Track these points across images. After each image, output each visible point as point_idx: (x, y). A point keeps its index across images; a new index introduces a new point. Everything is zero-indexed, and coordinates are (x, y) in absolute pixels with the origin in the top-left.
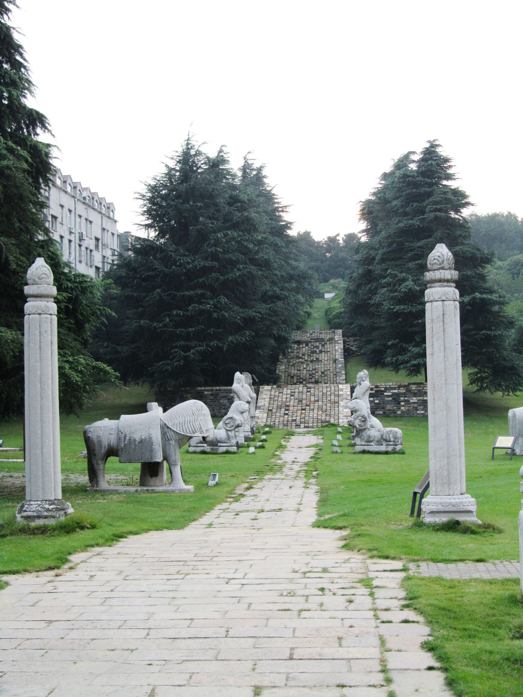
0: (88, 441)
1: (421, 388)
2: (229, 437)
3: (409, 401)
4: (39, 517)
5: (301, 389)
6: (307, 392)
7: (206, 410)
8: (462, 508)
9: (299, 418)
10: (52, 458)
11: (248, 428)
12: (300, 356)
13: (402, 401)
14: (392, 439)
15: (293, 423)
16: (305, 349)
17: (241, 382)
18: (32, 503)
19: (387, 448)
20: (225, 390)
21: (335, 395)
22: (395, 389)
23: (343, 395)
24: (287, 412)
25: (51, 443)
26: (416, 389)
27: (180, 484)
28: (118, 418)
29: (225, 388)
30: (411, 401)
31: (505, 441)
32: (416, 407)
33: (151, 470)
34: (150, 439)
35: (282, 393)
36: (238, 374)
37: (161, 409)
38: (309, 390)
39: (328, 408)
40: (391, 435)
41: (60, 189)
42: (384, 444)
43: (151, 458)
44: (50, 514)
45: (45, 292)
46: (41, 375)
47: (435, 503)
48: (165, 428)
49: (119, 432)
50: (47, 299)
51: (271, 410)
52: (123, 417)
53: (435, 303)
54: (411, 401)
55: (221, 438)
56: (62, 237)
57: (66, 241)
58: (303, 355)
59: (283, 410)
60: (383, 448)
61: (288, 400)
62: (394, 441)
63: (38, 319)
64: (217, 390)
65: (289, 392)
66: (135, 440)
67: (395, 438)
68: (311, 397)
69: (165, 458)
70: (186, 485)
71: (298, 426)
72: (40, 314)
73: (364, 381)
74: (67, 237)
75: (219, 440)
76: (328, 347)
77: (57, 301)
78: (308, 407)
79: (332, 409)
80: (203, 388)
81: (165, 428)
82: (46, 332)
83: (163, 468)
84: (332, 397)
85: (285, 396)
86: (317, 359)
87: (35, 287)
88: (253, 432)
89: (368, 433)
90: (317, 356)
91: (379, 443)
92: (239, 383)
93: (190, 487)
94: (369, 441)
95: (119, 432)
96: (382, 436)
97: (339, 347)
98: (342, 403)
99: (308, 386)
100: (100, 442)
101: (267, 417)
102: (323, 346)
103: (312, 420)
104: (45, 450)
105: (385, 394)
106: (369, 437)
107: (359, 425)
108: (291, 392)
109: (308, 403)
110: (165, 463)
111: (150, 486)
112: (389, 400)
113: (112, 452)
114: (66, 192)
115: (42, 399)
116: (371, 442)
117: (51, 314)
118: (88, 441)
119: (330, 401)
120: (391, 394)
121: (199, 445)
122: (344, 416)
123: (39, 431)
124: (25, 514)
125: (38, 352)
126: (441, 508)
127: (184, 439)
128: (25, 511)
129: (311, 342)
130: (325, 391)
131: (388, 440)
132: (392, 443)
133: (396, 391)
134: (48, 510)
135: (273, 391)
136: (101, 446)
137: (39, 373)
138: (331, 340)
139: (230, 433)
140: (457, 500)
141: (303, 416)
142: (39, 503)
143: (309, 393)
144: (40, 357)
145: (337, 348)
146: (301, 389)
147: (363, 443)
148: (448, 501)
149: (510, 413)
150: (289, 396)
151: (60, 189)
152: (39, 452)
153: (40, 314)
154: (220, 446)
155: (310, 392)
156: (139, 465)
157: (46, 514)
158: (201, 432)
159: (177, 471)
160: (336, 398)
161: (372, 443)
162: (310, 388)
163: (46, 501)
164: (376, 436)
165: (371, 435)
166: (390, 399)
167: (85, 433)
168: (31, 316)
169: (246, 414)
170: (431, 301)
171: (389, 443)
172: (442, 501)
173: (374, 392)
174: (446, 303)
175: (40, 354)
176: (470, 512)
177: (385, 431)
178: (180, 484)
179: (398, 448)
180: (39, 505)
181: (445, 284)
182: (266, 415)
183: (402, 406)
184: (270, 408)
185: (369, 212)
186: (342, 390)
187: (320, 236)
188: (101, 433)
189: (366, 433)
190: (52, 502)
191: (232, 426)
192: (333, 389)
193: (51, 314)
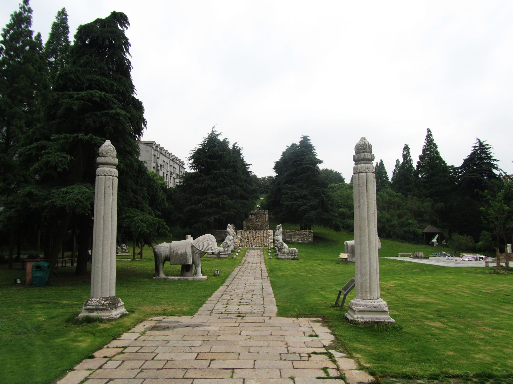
0: (155, 253)
2: (225, 251)
4: (97, 310)
7: (214, 239)
8: (380, 309)
10: (109, 269)
11: (232, 246)
17: (230, 229)
18: (94, 299)
25: (109, 260)
27: (200, 276)
28: (171, 242)
31: (344, 256)
33: (186, 268)
34: (186, 253)
36: (229, 225)
37: (192, 238)
41: (163, 155)
43: (186, 262)
44: (104, 307)
45: (110, 162)
46: (104, 214)
47: (362, 305)
48: (193, 248)
49: (170, 249)
50: (111, 166)
52: (173, 242)
53: (361, 174)
56: (164, 173)
57: (165, 175)
60: (290, 257)
63: (104, 179)
66: (178, 254)
67: (295, 252)
69: (193, 262)
70: (203, 275)
71: (252, 246)
72: (105, 175)
74: (166, 173)
76: (263, 216)
77: (118, 167)
81: (193, 248)
82: (109, 187)
83: (192, 269)
87: (103, 158)
88: (234, 248)
91: (288, 254)
93: (205, 277)
94: (284, 253)
95: (170, 249)
97: (267, 216)
98: (270, 237)
100: (161, 254)
104: (104, 264)
106: (284, 252)
110: (194, 265)
111: (186, 276)
113: (167, 259)
114: (166, 156)
115: (104, 230)
117: (113, 176)
118: (155, 253)
123: (101, 252)
124: (87, 307)
125: (103, 200)
126: (365, 308)
127: (202, 254)
128: (88, 305)
134: (103, 305)
136: (161, 256)
137: (103, 213)
138: (264, 213)
140: (376, 303)
142: (98, 299)
144: (104, 203)
148: (370, 304)
149: (345, 243)
151: (163, 155)
152: (100, 265)
153: (105, 175)
156: (181, 266)
157: (101, 307)
158: (212, 250)
159: (199, 269)
163: (103, 298)
167: (154, 249)
168: (100, 176)
169: (232, 241)
170: (358, 173)
172: (367, 303)
174: (368, 174)
175: (104, 201)
176: (384, 312)
178: (200, 276)
179: (296, 256)
180: (98, 301)
181: (367, 162)
185: (278, 167)
187: (259, 176)
188: (162, 250)
190: (107, 299)
193: (113, 176)
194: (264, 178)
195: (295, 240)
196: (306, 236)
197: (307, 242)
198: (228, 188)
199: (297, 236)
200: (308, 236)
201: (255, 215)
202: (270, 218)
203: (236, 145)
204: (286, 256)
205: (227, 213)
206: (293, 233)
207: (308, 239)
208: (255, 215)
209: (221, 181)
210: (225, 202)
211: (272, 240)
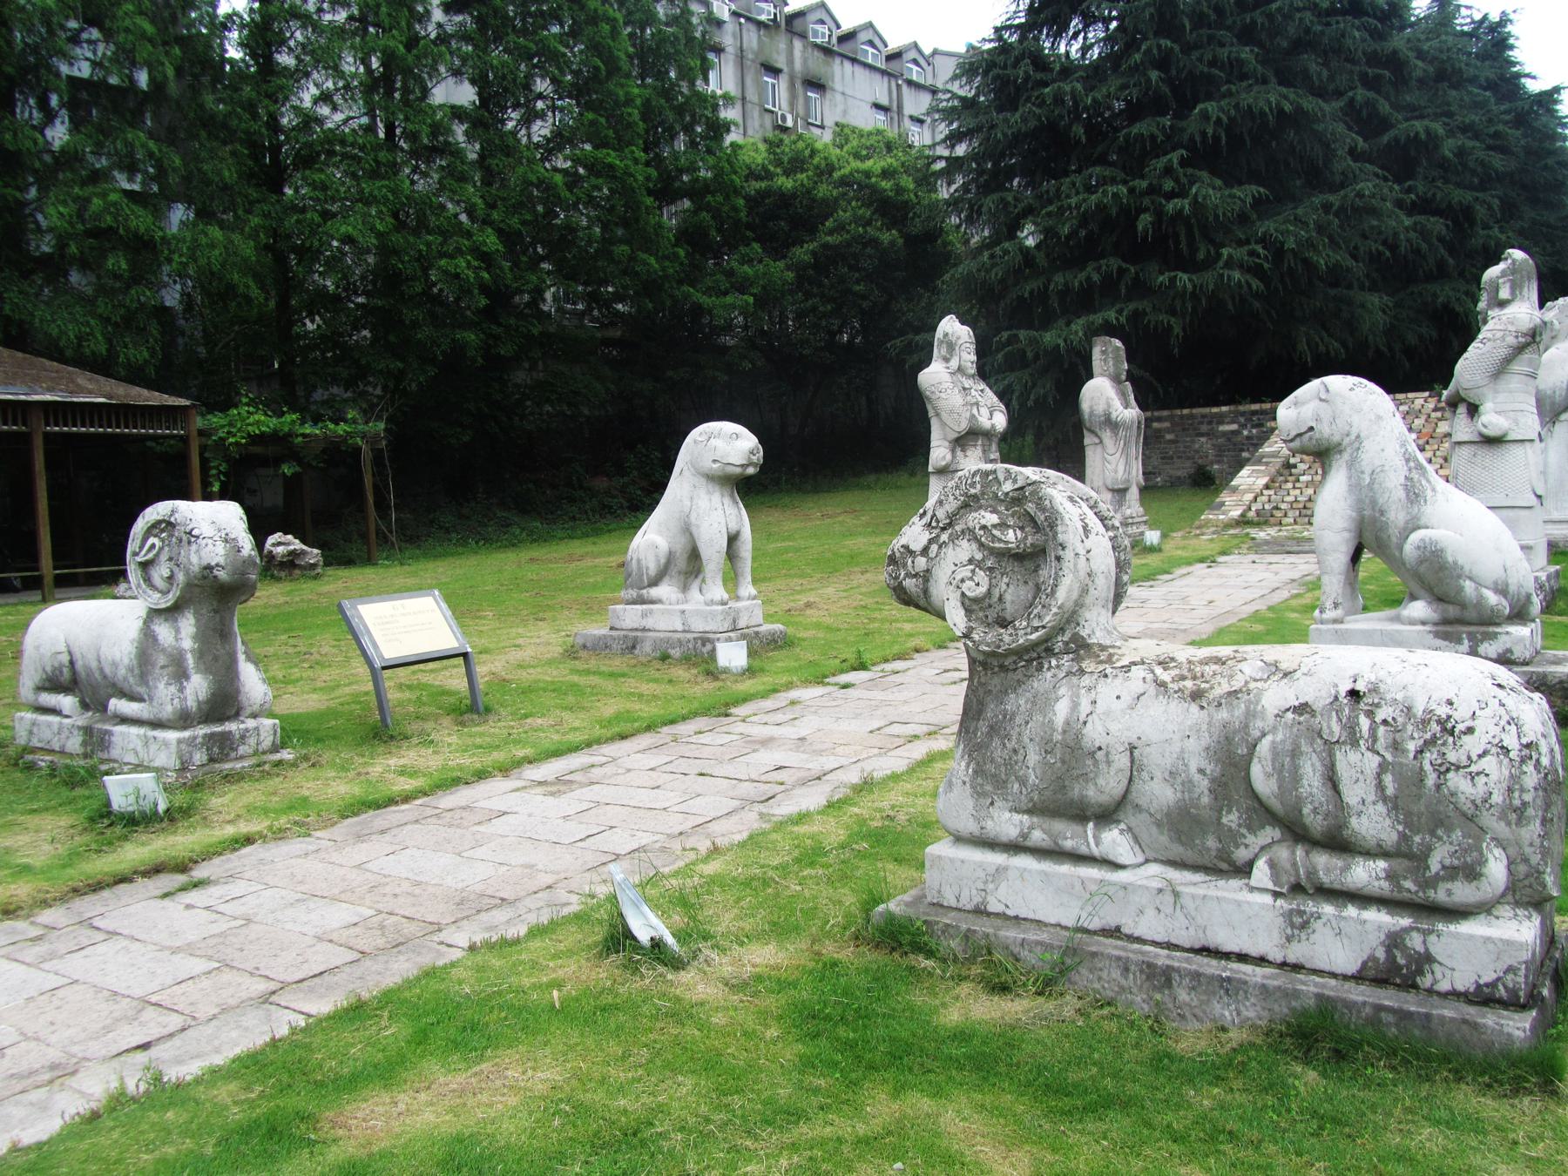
14: (1372, 823)
19: (1299, 925)
20: (1203, 416)
29: (1206, 410)
36: (951, 327)
40: (1357, 766)
42: (1261, 873)
55: (115, 664)
60: (1243, 913)
62: (1407, 856)
64: (1182, 417)
67: (1425, 808)
73: (1502, 304)
75: (108, 670)
89: (1061, 710)
92: (947, 360)
96: (1231, 759)
101: (1267, 487)
106: (1073, 753)
107: (971, 606)
116: (1106, 816)
121: (48, 699)
131: (1315, 822)
132: (1364, 873)
139: (163, 632)
147: (1007, 823)
154: (124, 720)
161: (1114, 841)
164: (1157, 759)
165: (1094, 734)
171: (1325, 865)
177: (1276, 697)
182: (1264, 481)
189: (1044, 703)
191: (171, 578)
198: (1211, 107)
204: (1139, 894)
205: (1183, 278)
209: (1163, 62)
210: (1171, 206)
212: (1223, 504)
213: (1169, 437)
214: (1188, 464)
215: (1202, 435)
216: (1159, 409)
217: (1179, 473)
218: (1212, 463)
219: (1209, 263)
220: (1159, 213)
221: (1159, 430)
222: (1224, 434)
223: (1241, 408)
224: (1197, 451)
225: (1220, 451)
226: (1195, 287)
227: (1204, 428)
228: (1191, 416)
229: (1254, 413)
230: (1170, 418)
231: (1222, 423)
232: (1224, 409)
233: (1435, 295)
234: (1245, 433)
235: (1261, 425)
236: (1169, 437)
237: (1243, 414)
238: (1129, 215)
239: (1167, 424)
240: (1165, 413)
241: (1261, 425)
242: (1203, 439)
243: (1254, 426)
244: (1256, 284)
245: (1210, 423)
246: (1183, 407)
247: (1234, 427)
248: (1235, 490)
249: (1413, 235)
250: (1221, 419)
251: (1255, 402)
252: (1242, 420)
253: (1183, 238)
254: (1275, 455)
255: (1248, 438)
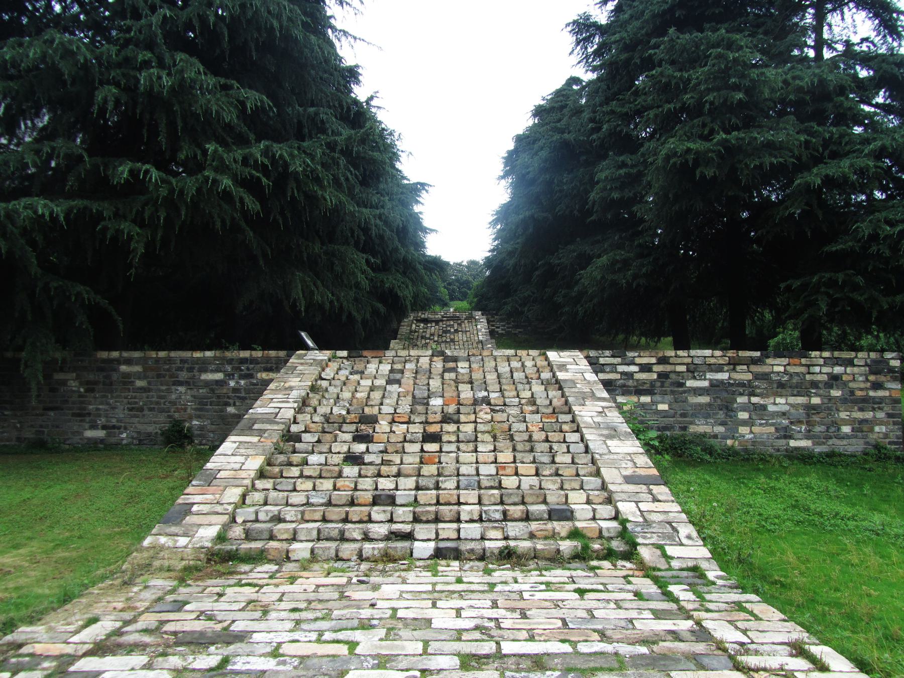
1: (803, 369)
3: (764, 407)
5: (424, 362)
6: (445, 370)
9: (411, 482)
12: (428, 336)
13: (744, 408)
15: (378, 513)
16: (433, 328)
20: (183, 361)
21: (546, 384)
22: (719, 369)
23: (573, 383)
24: (360, 447)
26: (786, 372)
29: (186, 354)
30: (771, 408)
32: (786, 428)
35: (362, 373)
38: (451, 365)
39: (538, 436)
51: (297, 438)
54: (771, 408)
58: (431, 335)
59: (348, 437)
61: (376, 396)
64: (157, 360)
65: (385, 368)
68: (462, 387)
78: (451, 428)
79: (554, 437)
80: (115, 354)
84: (538, 388)
85: (368, 383)
86: (453, 341)
90: (452, 337)
98: (587, 413)
99: (448, 353)
101: (262, 474)
102: (460, 325)
103: (470, 496)
105: (690, 383)
108: (392, 371)
109: (452, 409)
112: (700, 405)
119: (532, 401)
120: (706, 384)
122: (629, 480)
129: (442, 321)
130: (504, 368)
133: (724, 376)
135: (334, 365)
138: (470, 318)
141: (430, 469)
143: (453, 375)
145: (479, 327)
146: (424, 362)
150: (380, 382)
155: (454, 370)
160: (554, 393)
162: (455, 360)
166: (704, 400)
173: (655, 376)
182: (256, 463)
183: (744, 423)
184: (294, 428)
186: (563, 367)
192: (529, 364)
194: (460, 265)
195: (763, 430)
196: (852, 400)
197: (856, 446)
199: (779, 403)
200: (865, 403)
201: (437, 322)
202: (492, 333)
203: (373, 103)
206: (743, 375)
207: (861, 427)
208: (437, 322)
211: (633, 446)
212: (187, 510)
213: (140, 383)
214: (162, 417)
215: (181, 384)
216: (127, 349)
217: (150, 429)
218: (191, 418)
219: (195, 167)
220: (131, 89)
221: (127, 375)
222: (207, 384)
223: (228, 354)
224: (174, 403)
225: (202, 403)
226: (172, 191)
227: (184, 375)
228: (169, 360)
229: (243, 361)
230: (142, 361)
231: (206, 371)
232: (208, 354)
233: (382, 281)
234: (232, 384)
235: (251, 376)
236: (140, 383)
237: (230, 361)
238: (87, 79)
239: (138, 368)
240: (137, 354)
241: (251, 376)
242: (182, 389)
243: (242, 377)
244: (252, 204)
245: (191, 370)
246: (159, 349)
247: (219, 376)
248: (211, 479)
249: (378, 221)
250: (204, 366)
251: (244, 348)
252: (229, 368)
253: (162, 127)
254: (271, 419)
255: (235, 390)
